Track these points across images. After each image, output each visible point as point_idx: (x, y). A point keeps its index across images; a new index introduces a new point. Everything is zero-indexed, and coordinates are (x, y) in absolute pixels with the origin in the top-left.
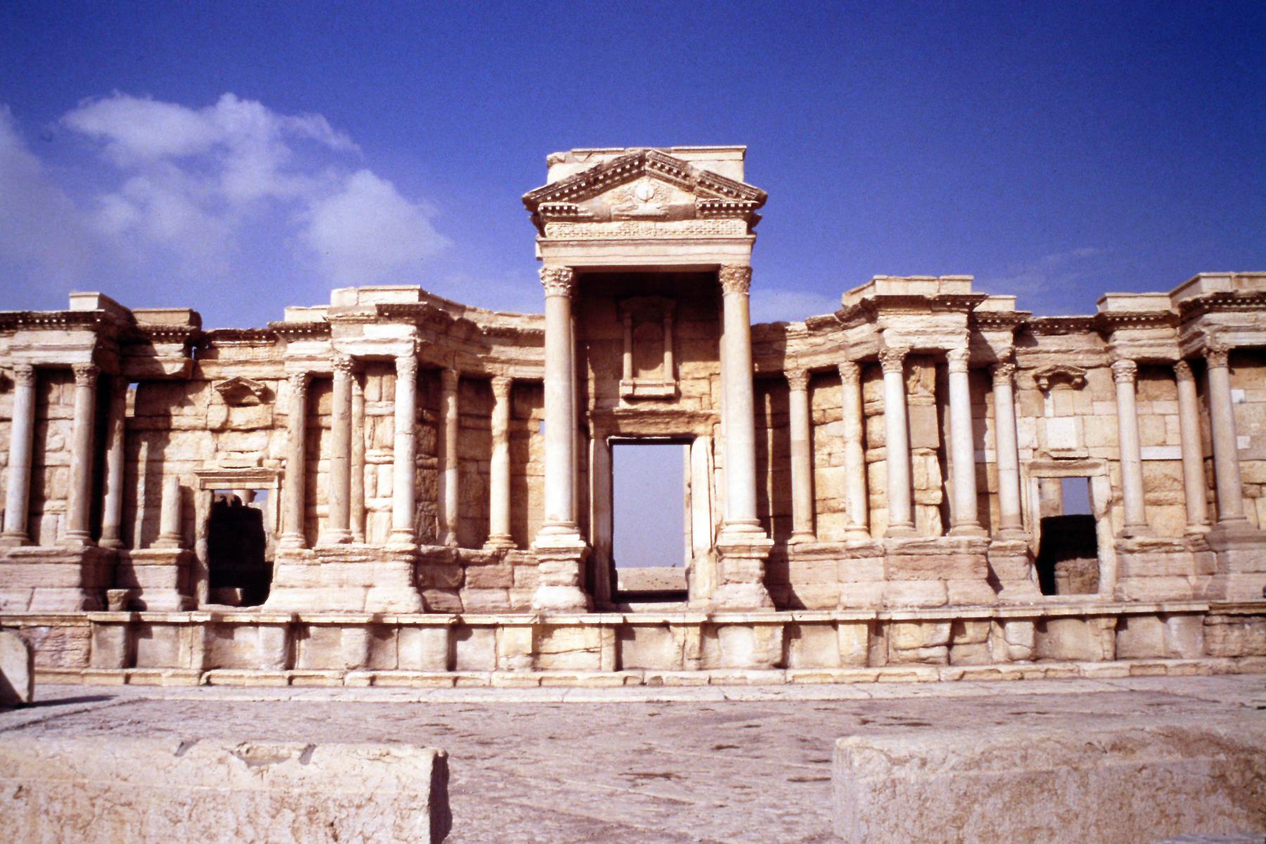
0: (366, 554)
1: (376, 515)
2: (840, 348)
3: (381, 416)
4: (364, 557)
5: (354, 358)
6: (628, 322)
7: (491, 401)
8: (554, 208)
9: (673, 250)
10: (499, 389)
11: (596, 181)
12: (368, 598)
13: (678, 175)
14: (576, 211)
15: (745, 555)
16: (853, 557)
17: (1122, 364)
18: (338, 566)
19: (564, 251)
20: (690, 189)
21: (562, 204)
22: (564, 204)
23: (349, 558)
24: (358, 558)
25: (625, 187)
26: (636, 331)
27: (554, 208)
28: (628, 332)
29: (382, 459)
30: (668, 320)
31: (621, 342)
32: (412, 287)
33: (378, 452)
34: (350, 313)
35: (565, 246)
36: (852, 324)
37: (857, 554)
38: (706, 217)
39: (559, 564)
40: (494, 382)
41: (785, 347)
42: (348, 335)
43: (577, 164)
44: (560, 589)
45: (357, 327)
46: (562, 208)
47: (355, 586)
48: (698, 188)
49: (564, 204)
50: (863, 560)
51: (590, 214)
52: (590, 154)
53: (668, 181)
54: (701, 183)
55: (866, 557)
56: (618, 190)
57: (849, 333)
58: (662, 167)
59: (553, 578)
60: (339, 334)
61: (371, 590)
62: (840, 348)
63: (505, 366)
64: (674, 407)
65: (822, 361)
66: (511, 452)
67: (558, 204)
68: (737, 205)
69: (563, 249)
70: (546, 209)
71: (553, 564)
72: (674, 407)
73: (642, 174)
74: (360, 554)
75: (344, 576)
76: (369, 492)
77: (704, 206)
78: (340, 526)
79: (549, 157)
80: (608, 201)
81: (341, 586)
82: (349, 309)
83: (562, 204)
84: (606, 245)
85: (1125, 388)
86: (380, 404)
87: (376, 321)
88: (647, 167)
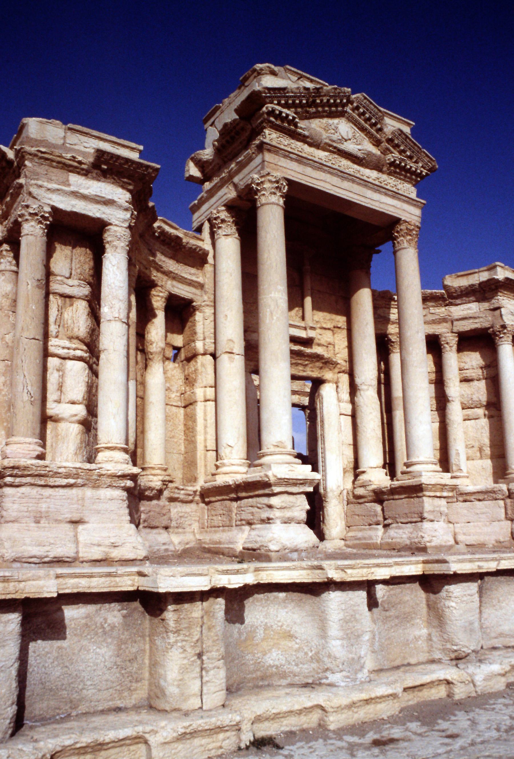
0: (77, 476)
1: (62, 425)
2: (444, 320)
3: (70, 297)
4: (72, 481)
5: (55, 210)
8: (281, 112)
9: (369, 193)
11: (313, 104)
12: (81, 538)
13: (370, 128)
14: (296, 125)
15: (438, 494)
16: (465, 501)
18: (34, 491)
19: (283, 162)
20: (377, 143)
21: (288, 112)
22: (290, 113)
23: (51, 481)
24: (64, 482)
25: (330, 121)
29: (72, 353)
32: (134, 145)
33: (67, 343)
34: (57, 152)
35: (285, 157)
36: (458, 301)
37: (472, 498)
38: (390, 174)
39: (291, 498)
40: (153, 292)
41: (389, 313)
42: (50, 180)
43: (289, 82)
44: (293, 526)
45: (57, 174)
46: (287, 115)
47: (57, 521)
48: (385, 145)
49: (290, 113)
50: (477, 503)
51: (306, 133)
52: (301, 77)
53: (362, 129)
54: (390, 141)
55: (480, 500)
56: (325, 120)
57: (453, 309)
58: (363, 114)
59: (288, 514)
60: (36, 175)
61: (81, 527)
62: (444, 320)
63: (165, 278)
64: (308, 351)
69: (282, 159)
70: (271, 113)
71: (285, 497)
72: (308, 351)
73: (341, 114)
74: (67, 476)
75: (43, 507)
76: (52, 395)
78: (33, 435)
79: (259, 66)
80: (315, 126)
81: (38, 522)
82: (55, 146)
83: (288, 112)
84: (319, 169)
86: (70, 282)
87: (86, 173)
88: (348, 109)
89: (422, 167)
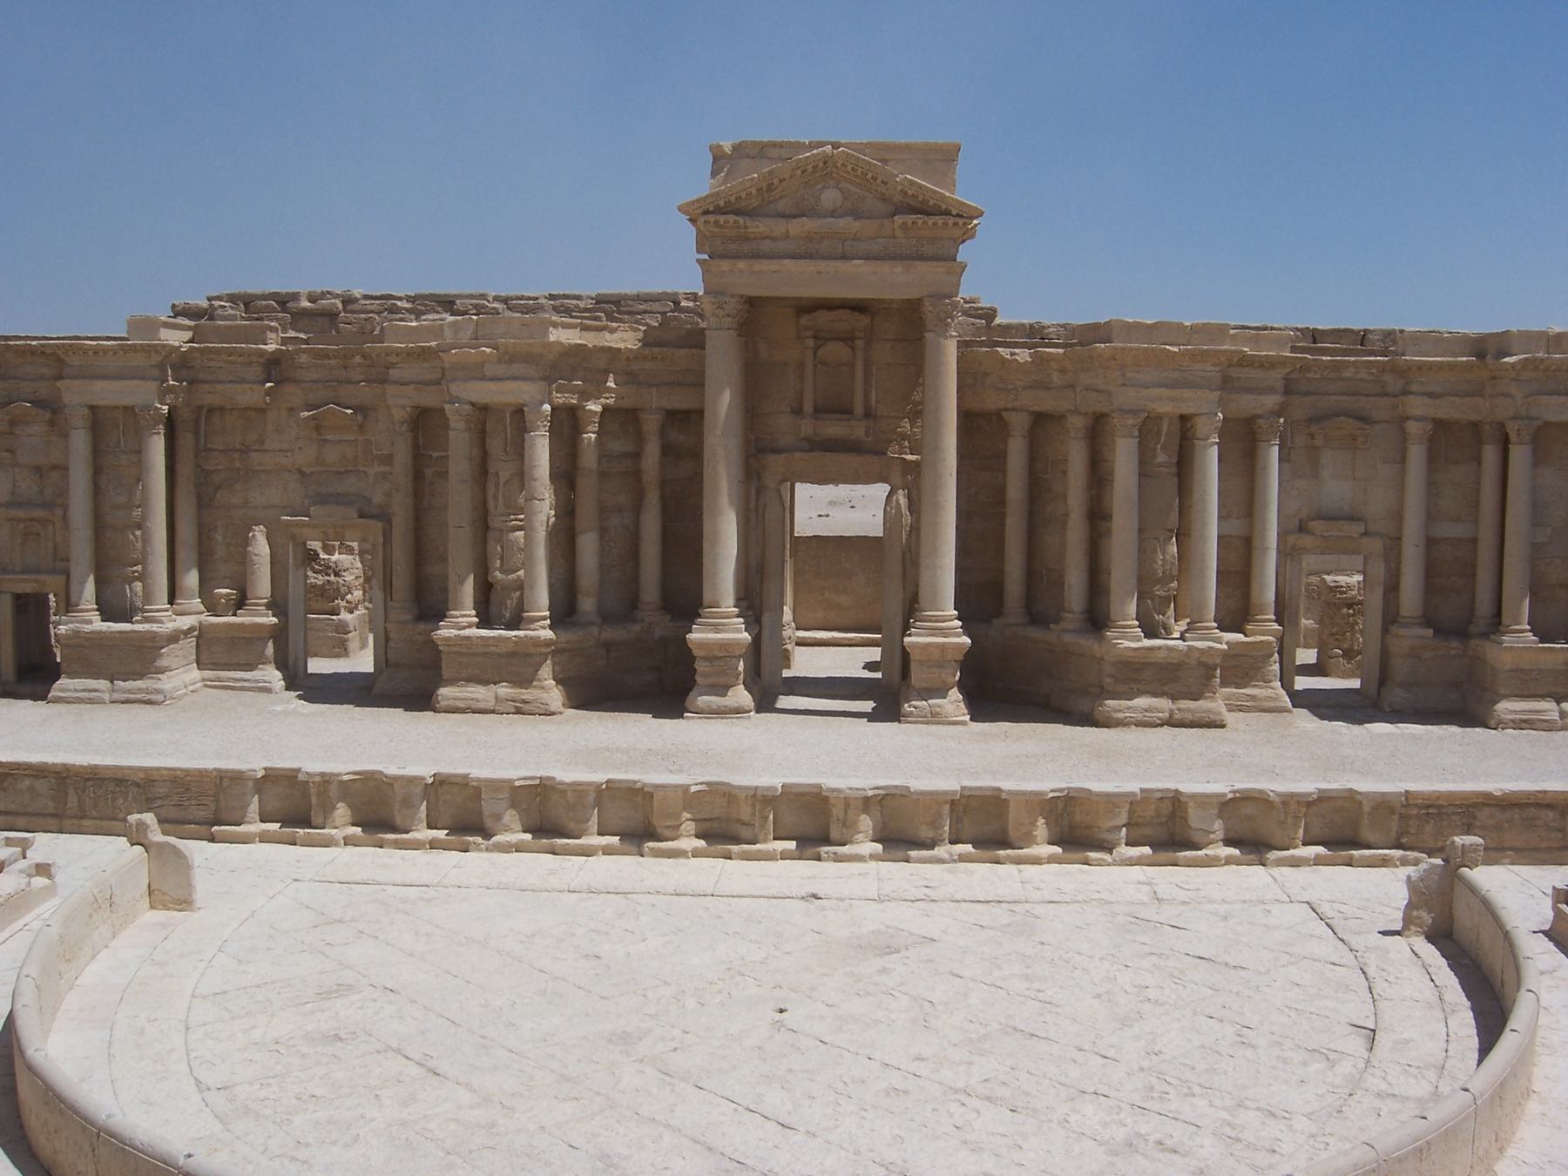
6: (811, 343)
7: (640, 438)
8: (716, 222)
10: (651, 424)
17: (1413, 427)
26: (820, 352)
27: (716, 222)
28: (810, 353)
30: (859, 343)
31: (801, 365)
65: (1046, 403)
66: (663, 497)
67: (722, 219)
68: (945, 224)
77: (904, 224)
85: (1417, 455)
87: (499, 361)
89: (958, 215)
